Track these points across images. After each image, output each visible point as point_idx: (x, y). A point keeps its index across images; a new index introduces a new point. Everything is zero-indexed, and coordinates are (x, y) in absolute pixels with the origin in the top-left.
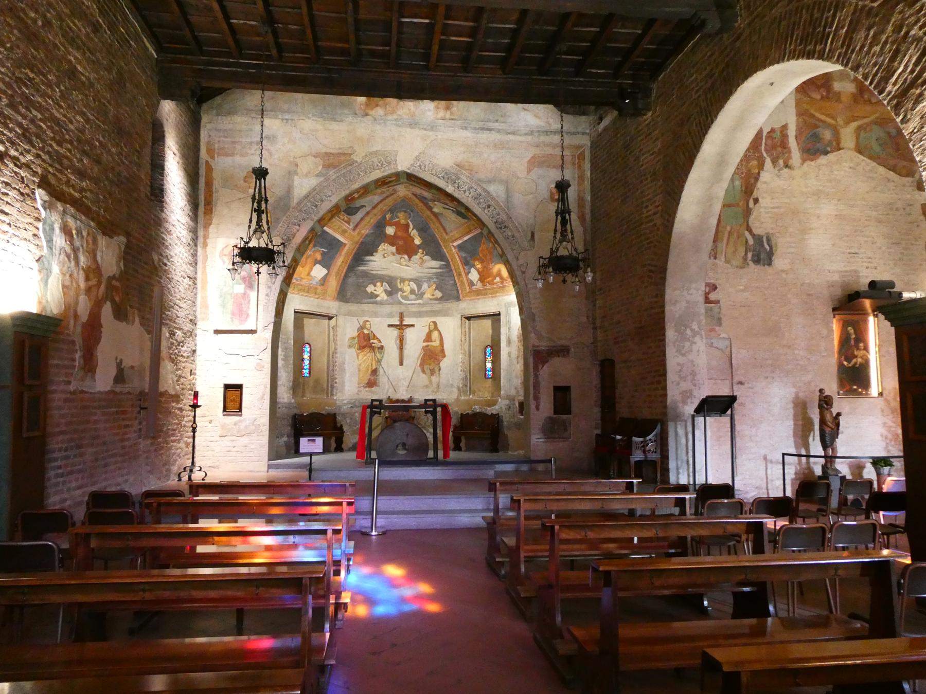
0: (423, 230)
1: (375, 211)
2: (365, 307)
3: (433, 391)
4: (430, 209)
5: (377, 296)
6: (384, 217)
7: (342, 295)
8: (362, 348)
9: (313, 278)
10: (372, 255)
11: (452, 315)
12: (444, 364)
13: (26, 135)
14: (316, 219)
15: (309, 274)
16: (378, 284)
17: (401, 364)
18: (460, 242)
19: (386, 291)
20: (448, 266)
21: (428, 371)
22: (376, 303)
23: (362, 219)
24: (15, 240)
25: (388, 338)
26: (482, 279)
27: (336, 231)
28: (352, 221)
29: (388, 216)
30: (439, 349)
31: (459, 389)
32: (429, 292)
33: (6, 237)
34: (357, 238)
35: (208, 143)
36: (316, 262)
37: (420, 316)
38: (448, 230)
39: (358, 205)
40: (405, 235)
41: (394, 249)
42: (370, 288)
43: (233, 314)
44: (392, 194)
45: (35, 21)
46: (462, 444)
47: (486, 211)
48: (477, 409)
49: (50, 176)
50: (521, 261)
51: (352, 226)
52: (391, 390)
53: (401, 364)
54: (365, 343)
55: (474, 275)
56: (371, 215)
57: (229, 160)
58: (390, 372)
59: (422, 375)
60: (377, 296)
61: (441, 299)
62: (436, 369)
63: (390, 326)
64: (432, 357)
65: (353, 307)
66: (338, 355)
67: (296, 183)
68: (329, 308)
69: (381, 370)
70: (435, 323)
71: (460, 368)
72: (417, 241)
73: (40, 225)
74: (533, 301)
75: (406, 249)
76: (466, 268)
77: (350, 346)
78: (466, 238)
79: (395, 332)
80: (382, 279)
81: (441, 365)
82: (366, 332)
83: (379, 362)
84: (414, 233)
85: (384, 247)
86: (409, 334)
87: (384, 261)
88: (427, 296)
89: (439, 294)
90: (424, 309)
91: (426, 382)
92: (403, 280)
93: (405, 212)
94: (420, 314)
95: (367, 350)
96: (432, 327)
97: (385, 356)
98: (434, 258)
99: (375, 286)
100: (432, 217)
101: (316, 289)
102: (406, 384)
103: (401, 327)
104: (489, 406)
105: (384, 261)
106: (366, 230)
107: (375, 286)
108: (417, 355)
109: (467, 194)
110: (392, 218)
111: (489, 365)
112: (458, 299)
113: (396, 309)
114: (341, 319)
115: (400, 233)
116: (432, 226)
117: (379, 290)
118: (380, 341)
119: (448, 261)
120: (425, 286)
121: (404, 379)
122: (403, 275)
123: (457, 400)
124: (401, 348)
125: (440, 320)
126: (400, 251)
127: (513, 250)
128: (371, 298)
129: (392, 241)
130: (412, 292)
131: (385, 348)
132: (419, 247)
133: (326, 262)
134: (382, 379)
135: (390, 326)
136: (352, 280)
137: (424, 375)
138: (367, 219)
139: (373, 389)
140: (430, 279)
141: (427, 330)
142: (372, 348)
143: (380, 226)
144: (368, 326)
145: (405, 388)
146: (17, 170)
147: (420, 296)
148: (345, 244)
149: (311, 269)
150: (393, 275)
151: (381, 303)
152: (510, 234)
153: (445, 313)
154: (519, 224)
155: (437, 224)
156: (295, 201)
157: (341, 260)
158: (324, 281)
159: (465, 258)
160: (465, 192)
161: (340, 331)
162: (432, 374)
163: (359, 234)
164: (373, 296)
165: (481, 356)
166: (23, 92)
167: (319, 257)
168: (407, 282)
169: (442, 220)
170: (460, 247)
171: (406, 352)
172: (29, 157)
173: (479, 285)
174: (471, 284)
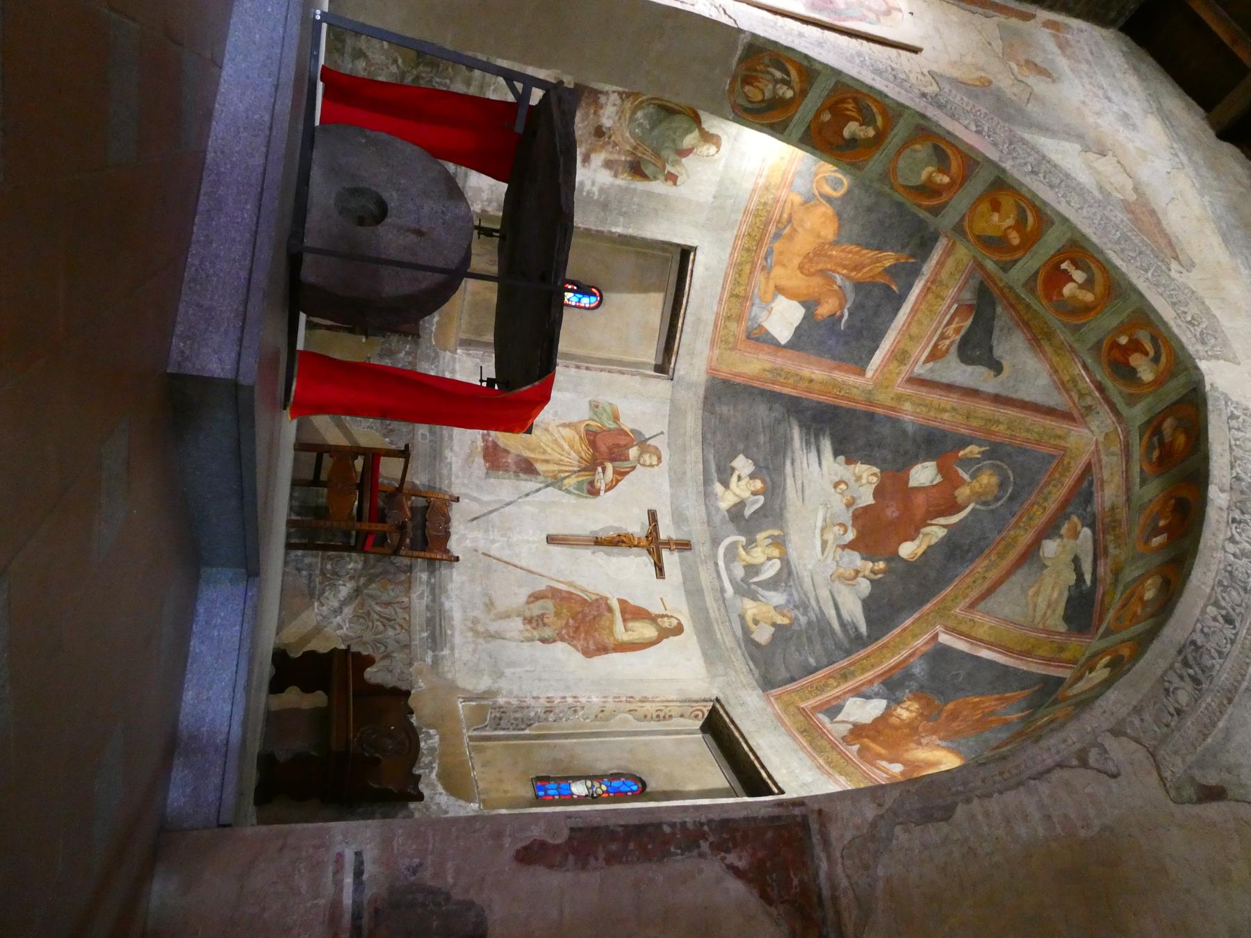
0: (956, 551)
1: (985, 409)
2: (695, 453)
3: (475, 621)
4: (1051, 529)
5: (726, 484)
6: (964, 442)
7: (722, 391)
8: (592, 437)
9: (767, 306)
10: (836, 454)
11: (713, 676)
12: (565, 655)
14: (1008, 165)
15: (779, 290)
16: (758, 484)
17: (551, 540)
18: (961, 645)
19: (741, 504)
20: (858, 642)
21: (536, 609)
22: (707, 482)
23: (949, 388)
25: (622, 509)
26: (858, 731)
27: (905, 331)
28: (937, 365)
29: (973, 450)
30: (610, 642)
31: (490, 694)
32: (765, 612)
34: (883, 397)
35: (1067, 27)
36: (810, 305)
37: (689, 593)
38: (990, 603)
39: (998, 352)
40: (919, 513)
41: (867, 499)
42: (743, 465)
44: (1067, 416)
46: (293, 697)
47: (1212, 610)
48: (430, 741)
50: (1119, 750)
51: (920, 370)
52: (476, 509)
53: (551, 540)
54: (603, 449)
55: (865, 711)
56: (969, 404)
57: (1051, 46)
58: (528, 508)
59: (523, 594)
60: (726, 484)
61: (749, 642)
62: (547, 632)
63: (652, 515)
64: (583, 621)
65: (692, 422)
66: (573, 371)
67: (1067, 145)
68: (692, 354)
69: (531, 485)
70: (678, 630)
71: (556, 695)
72: (907, 550)
74: (994, 805)
75: (872, 531)
76: (876, 687)
77: (594, 406)
78: (985, 654)
79: (637, 527)
80: (773, 490)
81: (560, 645)
82: (633, 452)
83: (556, 482)
84: (935, 532)
85: (864, 480)
86: (636, 565)
87: (827, 486)
88: (751, 608)
89: (763, 635)
90: (711, 603)
91: (502, 604)
92: (779, 542)
93: (1002, 485)
94: (693, 591)
95: (586, 452)
96: (666, 623)
97: (572, 500)
98: (867, 604)
99: (752, 476)
100: (1012, 556)
101: (739, 318)
102: (495, 550)
103: (653, 544)
104: (445, 778)
105: (827, 486)
106: (912, 412)
107: (752, 476)
108: (582, 582)
109: (1231, 548)
110: (967, 463)
111: (579, 789)
112: (767, 683)
113: (697, 532)
114: (661, 386)
115: (920, 500)
116: (980, 565)
117: (743, 487)
118: (609, 488)
119: (872, 638)
120: (778, 598)
121: (510, 546)
122: (795, 540)
123: (453, 688)
124: (598, 542)
125: (689, 636)
126: (863, 518)
127: (1137, 710)
128: (719, 470)
129: (893, 486)
130: (752, 569)
131: (592, 501)
132: (894, 557)
133: (809, 337)
134: (505, 488)
135: (652, 515)
136: (762, 412)
137: (523, 598)
138: (951, 401)
139: (479, 460)
140: (804, 606)
141: (656, 609)
142: (592, 465)
143: (933, 443)
144: (647, 458)
145: (482, 545)
147: (745, 589)
148: (862, 373)
149: (791, 295)
150: (790, 514)
151: (708, 495)
152: (1183, 698)
153: (712, 653)
154: (1227, 736)
155: (994, 575)
156: (1027, 136)
157: (817, 376)
158: (760, 338)
159: (909, 676)
160: (1232, 539)
161: (634, 382)
162: (529, 621)
163: (899, 398)
164: (725, 476)
165: (604, 766)
167: (825, 309)
168: (776, 553)
169: (1018, 578)
170: (941, 655)
171: (586, 554)
173: (837, 728)
174: (833, 710)
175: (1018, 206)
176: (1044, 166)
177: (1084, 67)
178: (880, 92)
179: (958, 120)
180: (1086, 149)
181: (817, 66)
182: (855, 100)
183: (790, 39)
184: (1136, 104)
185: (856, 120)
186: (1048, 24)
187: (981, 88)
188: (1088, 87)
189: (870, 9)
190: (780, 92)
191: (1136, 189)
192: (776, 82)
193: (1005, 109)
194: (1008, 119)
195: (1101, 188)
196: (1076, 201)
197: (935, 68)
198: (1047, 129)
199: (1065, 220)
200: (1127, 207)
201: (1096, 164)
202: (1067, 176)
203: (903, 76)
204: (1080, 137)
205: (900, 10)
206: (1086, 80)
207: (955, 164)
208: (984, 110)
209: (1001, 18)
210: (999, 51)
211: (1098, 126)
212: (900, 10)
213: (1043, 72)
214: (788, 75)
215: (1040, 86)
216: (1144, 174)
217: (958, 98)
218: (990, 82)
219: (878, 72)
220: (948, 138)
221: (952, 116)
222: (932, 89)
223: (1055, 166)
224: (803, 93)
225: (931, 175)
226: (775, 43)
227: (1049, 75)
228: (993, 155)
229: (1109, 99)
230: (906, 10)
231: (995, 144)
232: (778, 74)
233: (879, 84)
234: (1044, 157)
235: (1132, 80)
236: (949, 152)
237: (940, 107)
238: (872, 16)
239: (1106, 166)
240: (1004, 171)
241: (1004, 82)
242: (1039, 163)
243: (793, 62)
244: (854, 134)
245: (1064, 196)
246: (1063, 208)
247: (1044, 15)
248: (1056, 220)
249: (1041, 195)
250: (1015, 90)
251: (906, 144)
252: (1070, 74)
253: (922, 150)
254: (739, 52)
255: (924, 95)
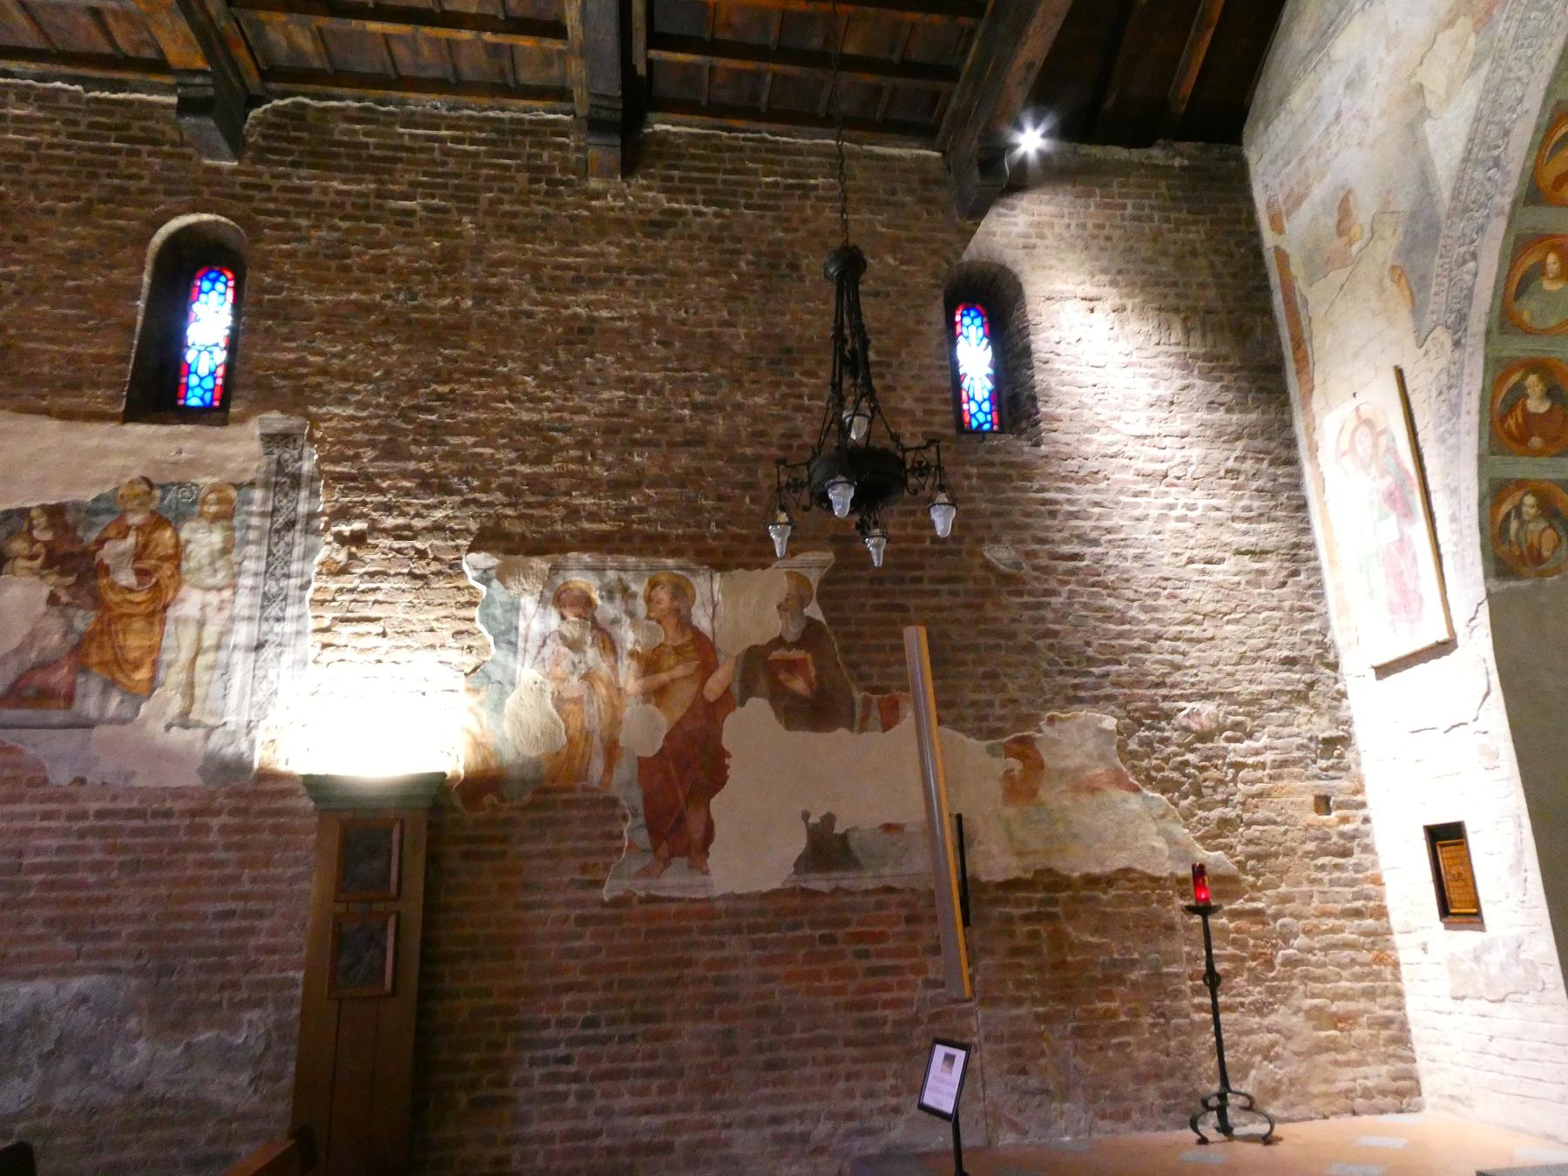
13: (431, 484)
14: (1505, 202)
24: (401, 655)
33: (373, 656)
35: (1269, 205)
43: (1393, 609)
45: (455, 307)
49: (506, 524)
57: (1304, 213)
67: (1432, 141)
73: (475, 612)
146: (403, 544)
156: (1446, 194)
166: (424, 424)
172: (438, 514)
175: (1552, 154)
176: (1480, 150)
177: (1310, 163)
178: (1482, 398)
179: (1471, 289)
180: (1424, 113)
181: (1486, 485)
182: (1503, 419)
183: (1467, 532)
184: (1326, 81)
185: (1524, 407)
186: (1278, 228)
187: (1410, 275)
188: (1335, 148)
189: (1375, 446)
190: (1533, 511)
191: (1450, 24)
192: (1523, 523)
193: (1421, 235)
194: (1433, 226)
195: (1474, 68)
196: (1511, 93)
197: (1410, 341)
198: (1423, 172)
199: (1549, 92)
200: (1484, 22)
201: (1441, 92)
202: (1477, 119)
203: (1444, 378)
204: (1413, 130)
205: (1357, 409)
206: (1329, 154)
207: (1530, 261)
208: (1438, 261)
209: (1300, 284)
210: (1343, 274)
211: (1383, 113)
212: (1357, 409)
213: (1344, 210)
214: (1508, 515)
215: (1366, 207)
216: (1419, 26)
217: (1437, 300)
218: (1393, 268)
219: (1454, 409)
220: (1500, 293)
221: (1469, 297)
222: (1443, 337)
223: (1471, 140)
224: (1521, 484)
225: (1553, 279)
226: (1483, 548)
227: (1345, 200)
228: (1498, 227)
229: (1338, 115)
230: (1350, 406)
231: (1481, 229)
232: (1514, 525)
233: (1471, 405)
234: (1465, 160)
235: (1296, 99)
236: (1517, 278)
237: (1463, 318)
238: (1383, 441)
239: (1435, 79)
240: (1515, 203)
241: (1386, 249)
242: (1477, 162)
243: (1493, 515)
244: (1541, 398)
245: (1512, 109)
246: (1534, 101)
247: (1269, 238)
248: (1553, 102)
249: (1527, 139)
250: (1389, 233)
251: (1528, 331)
252: (1329, 178)
253: (1528, 310)
254: (1512, 584)
255: (1457, 344)
